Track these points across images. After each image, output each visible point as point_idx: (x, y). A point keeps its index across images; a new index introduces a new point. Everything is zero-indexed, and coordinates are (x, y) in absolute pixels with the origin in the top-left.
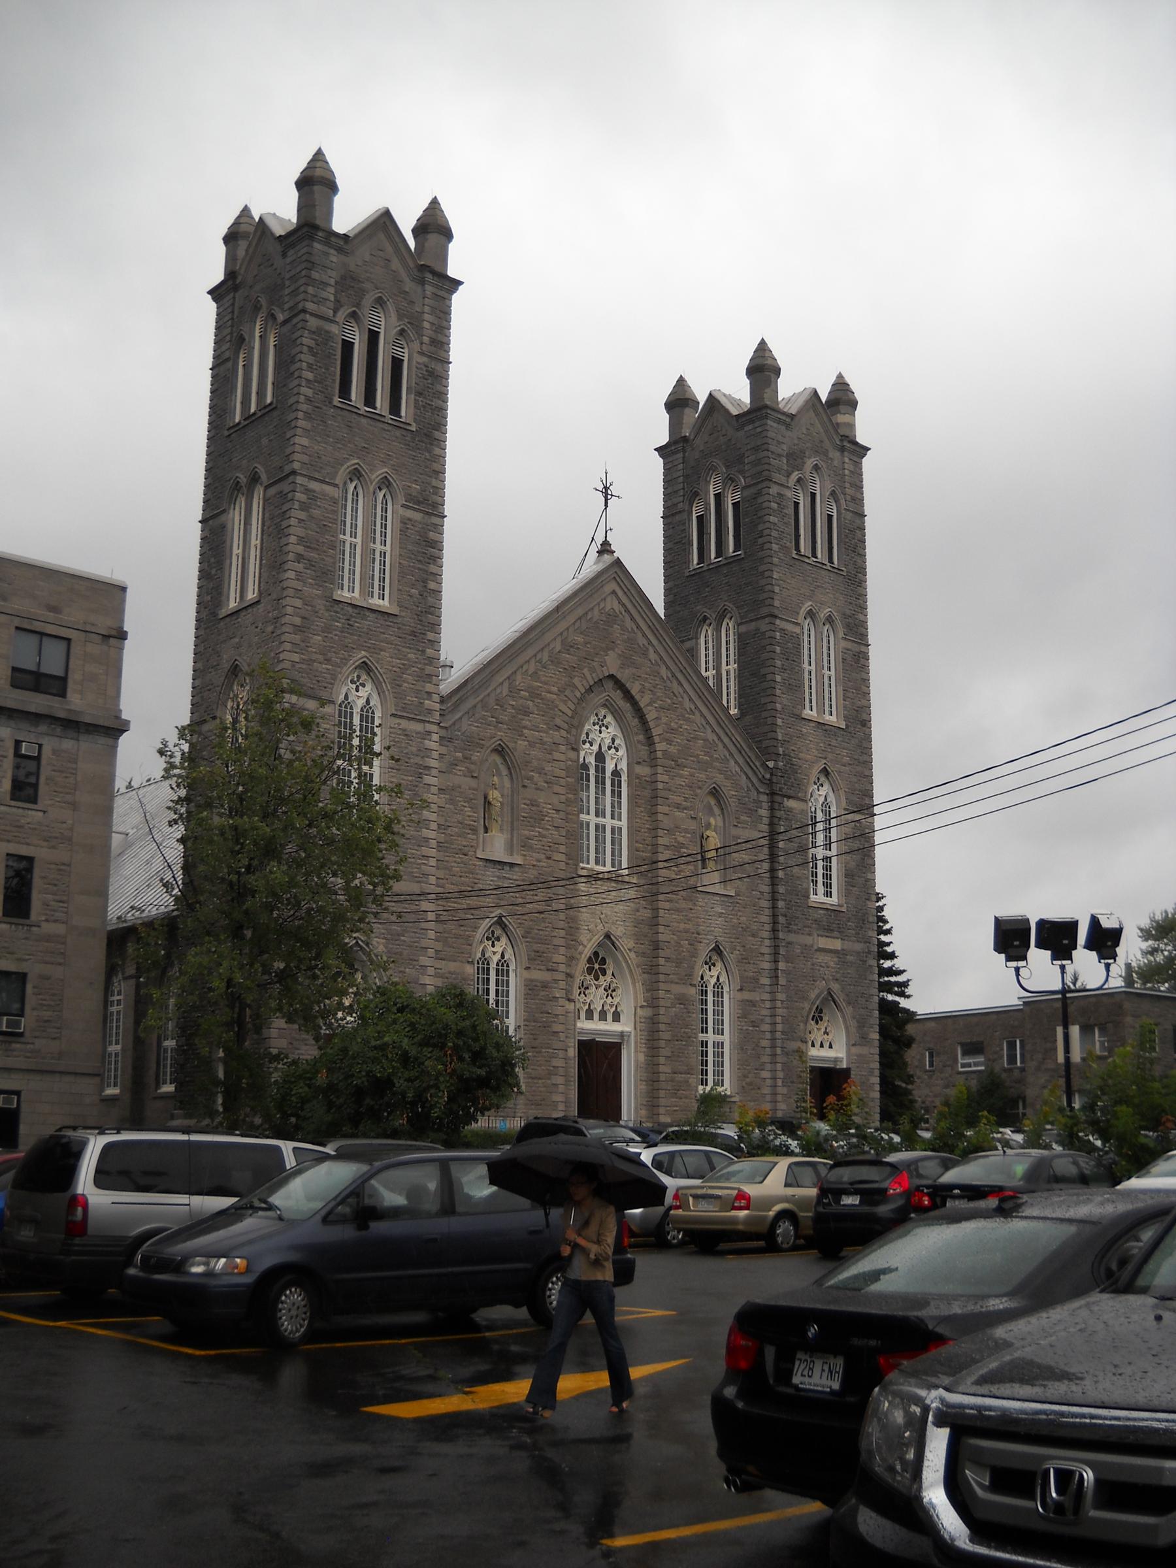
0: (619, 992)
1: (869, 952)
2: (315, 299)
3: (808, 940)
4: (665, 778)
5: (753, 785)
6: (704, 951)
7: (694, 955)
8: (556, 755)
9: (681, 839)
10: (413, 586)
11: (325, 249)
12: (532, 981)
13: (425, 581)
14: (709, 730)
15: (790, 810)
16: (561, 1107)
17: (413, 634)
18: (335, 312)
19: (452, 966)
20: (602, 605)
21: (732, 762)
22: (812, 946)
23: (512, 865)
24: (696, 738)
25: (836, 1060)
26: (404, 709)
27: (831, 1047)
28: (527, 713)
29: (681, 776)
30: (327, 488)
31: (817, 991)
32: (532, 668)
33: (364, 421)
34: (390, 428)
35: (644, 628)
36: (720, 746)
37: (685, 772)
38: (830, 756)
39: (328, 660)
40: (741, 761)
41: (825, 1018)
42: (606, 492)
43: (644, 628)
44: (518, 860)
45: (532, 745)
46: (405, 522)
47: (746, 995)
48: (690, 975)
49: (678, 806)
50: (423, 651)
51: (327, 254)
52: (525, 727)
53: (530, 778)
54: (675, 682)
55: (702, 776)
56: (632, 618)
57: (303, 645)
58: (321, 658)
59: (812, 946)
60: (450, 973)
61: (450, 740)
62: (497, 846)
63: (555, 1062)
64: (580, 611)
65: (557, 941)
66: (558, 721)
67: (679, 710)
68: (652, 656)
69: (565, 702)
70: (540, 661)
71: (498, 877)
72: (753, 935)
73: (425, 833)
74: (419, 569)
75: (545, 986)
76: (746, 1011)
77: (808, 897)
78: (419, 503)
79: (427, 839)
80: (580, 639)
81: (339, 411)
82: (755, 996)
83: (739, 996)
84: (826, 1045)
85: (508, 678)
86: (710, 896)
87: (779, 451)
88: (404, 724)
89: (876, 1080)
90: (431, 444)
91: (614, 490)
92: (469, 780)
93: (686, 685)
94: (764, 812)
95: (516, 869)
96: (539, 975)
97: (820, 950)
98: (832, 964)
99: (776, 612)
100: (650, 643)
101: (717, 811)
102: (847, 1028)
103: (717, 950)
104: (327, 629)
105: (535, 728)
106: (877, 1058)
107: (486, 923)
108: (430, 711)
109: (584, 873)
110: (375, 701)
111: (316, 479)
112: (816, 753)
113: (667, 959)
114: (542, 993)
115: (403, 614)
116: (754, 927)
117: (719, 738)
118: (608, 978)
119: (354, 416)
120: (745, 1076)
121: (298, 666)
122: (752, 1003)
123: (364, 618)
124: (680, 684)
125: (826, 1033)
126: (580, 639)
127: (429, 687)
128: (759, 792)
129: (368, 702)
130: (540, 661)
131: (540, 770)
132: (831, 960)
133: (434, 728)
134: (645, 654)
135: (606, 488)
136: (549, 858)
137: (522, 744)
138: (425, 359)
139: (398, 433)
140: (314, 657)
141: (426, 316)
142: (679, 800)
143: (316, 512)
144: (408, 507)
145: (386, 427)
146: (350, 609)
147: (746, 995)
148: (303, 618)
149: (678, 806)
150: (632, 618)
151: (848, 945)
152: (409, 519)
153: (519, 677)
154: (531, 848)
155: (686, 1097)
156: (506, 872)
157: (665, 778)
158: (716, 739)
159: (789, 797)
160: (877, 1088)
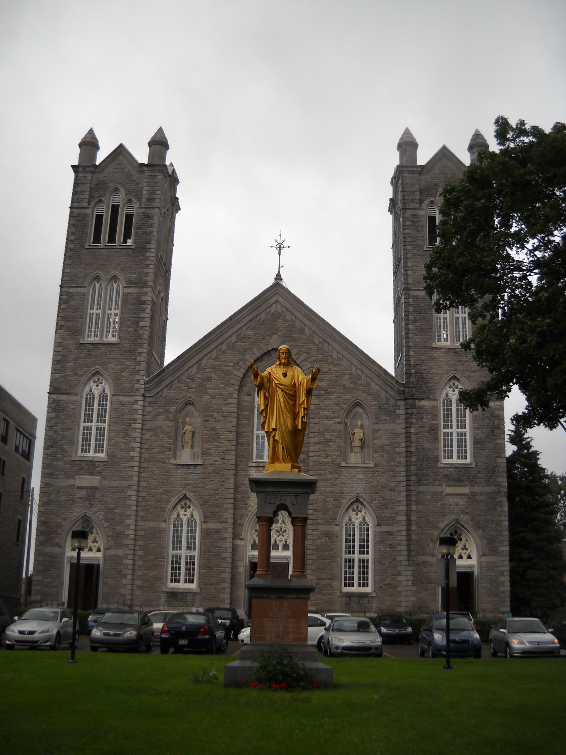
0: (287, 532)
1: (499, 492)
2: (78, 201)
3: (439, 489)
4: (317, 402)
5: (391, 396)
6: (345, 503)
7: (339, 506)
8: (230, 400)
9: (328, 437)
10: (130, 327)
11: (85, 175)
12: (208, 529)
13: (138, 323)
14: (354, 368)
15: (421, 407)
16: (228, 601)
17: (130, 351)
18: (89, 203)
19: (152, 524)
20: (268, 311)
21: (373, 385)
22: (442, 492)
23: (195, 466)
24: (343, 375)
25: (471, 566)
26: (121, 391)
27: (469, 557)
28: (210, 380)
29: (330, 399)
30: (80, 290)
31: (446, 522)
32: (214, 354)
33: (103, 251)
34: (119, 250)
35: (301, 317)
36: (363, 376)
37: (334, 396)
38: (460, 368)
39: (76, 374)
40: (380, 383)
41: (464, 539)
42: (280, 247)
43: (301, 317)
44: (200, 462)
45: (213, 397)
46: (125, 295)
47: (384, 528)
48: (335, 519)
49: (327, 417)
50: (135, 359)
51: (85, 177)
52: (208, 388)
53: (212, 416)
54: (326, 344)
55: (348, 396)
56: (292, 314)
57: (62, 369)
58: (72, 373)
59: (442, 492)
60: (150, 528)
61: (155, 403)
62: (185, 456)
63: (222, 575)
64: (251, 317)
65: (226, 506)
66: (232, 381)
67: (330, 360)
68: (307, 331)
69: (238, 370)
70: (220, 350)
71: (186, 473)
72: (391, 490)
73: (132, 454)
74: (134, 317)
75: (217, 531)
76: (383, 539)
77: (437, 460)
78: (135, 283)
79: (133, 458)
80: (251, 333)
81: (89, 250)
82: (394, 529)
83: (378, 529)
84: (465, 557)
85: (197, 362)
86: (352, 469)
87: (414, 189)
88: (121, 399)
89: (506, 579)
90: (145, 252)
91: (285, 244)
92: (167, 422)
93: (334, 344)
94: (401, 412)
95: (199, 467)
96: (212, 526)
97: (447, 494)
98: (462, 503)
99: (409, 286)
100: (305, 325)
101: (364, 416)
102: (476, 544)
103: (357, 501)
104: (77, 359)
105: (217, 387)
106: (507, 563)
107: (175, 500)
108: (138, 390)
109: (254, 465)
110: (108, 391)
111: (72, 287)
112: (447, 368)
113: (315, 510)
114: (215, 536)
115: (122, 342)
116: (392, 485)
117: (362, 372)
118: (278, 525)
119: (98, 250)
120: (383, 580)
121: (58, 380)
122: (390, 533)
123: (99, 349)
124: (329, 344)
125: (465, 548)
126: (251, 333)
127: (137, 377)
128: (396, 400)
129: (104, 391)
130: (220, 350)
131: (219, 411)
132: (462, 501)
133: (141, 398)
134: (302, 332)
135: (280, 244)
136: (223, 459)
137: (206, 398)
138: (143, 210)
139: (124, 251)
140: (68, 373)
141: (145, 188)
142: (328, 413)
143: (72, 303)
144: (128, 287)
145: (117, 250)
146: (90, 346)
147: (384, 528)
148: (63, 356)
149: (327, 417)
150: (292, 314)
151: (476, 489)
152: (129, 293)
153: (204, 362)
154: (210, 454)
155: (329, 594)
156: (191, 470)
157: (317, 402)
158: (359, 372)
159: (421, 399)
160: (508, 584)
